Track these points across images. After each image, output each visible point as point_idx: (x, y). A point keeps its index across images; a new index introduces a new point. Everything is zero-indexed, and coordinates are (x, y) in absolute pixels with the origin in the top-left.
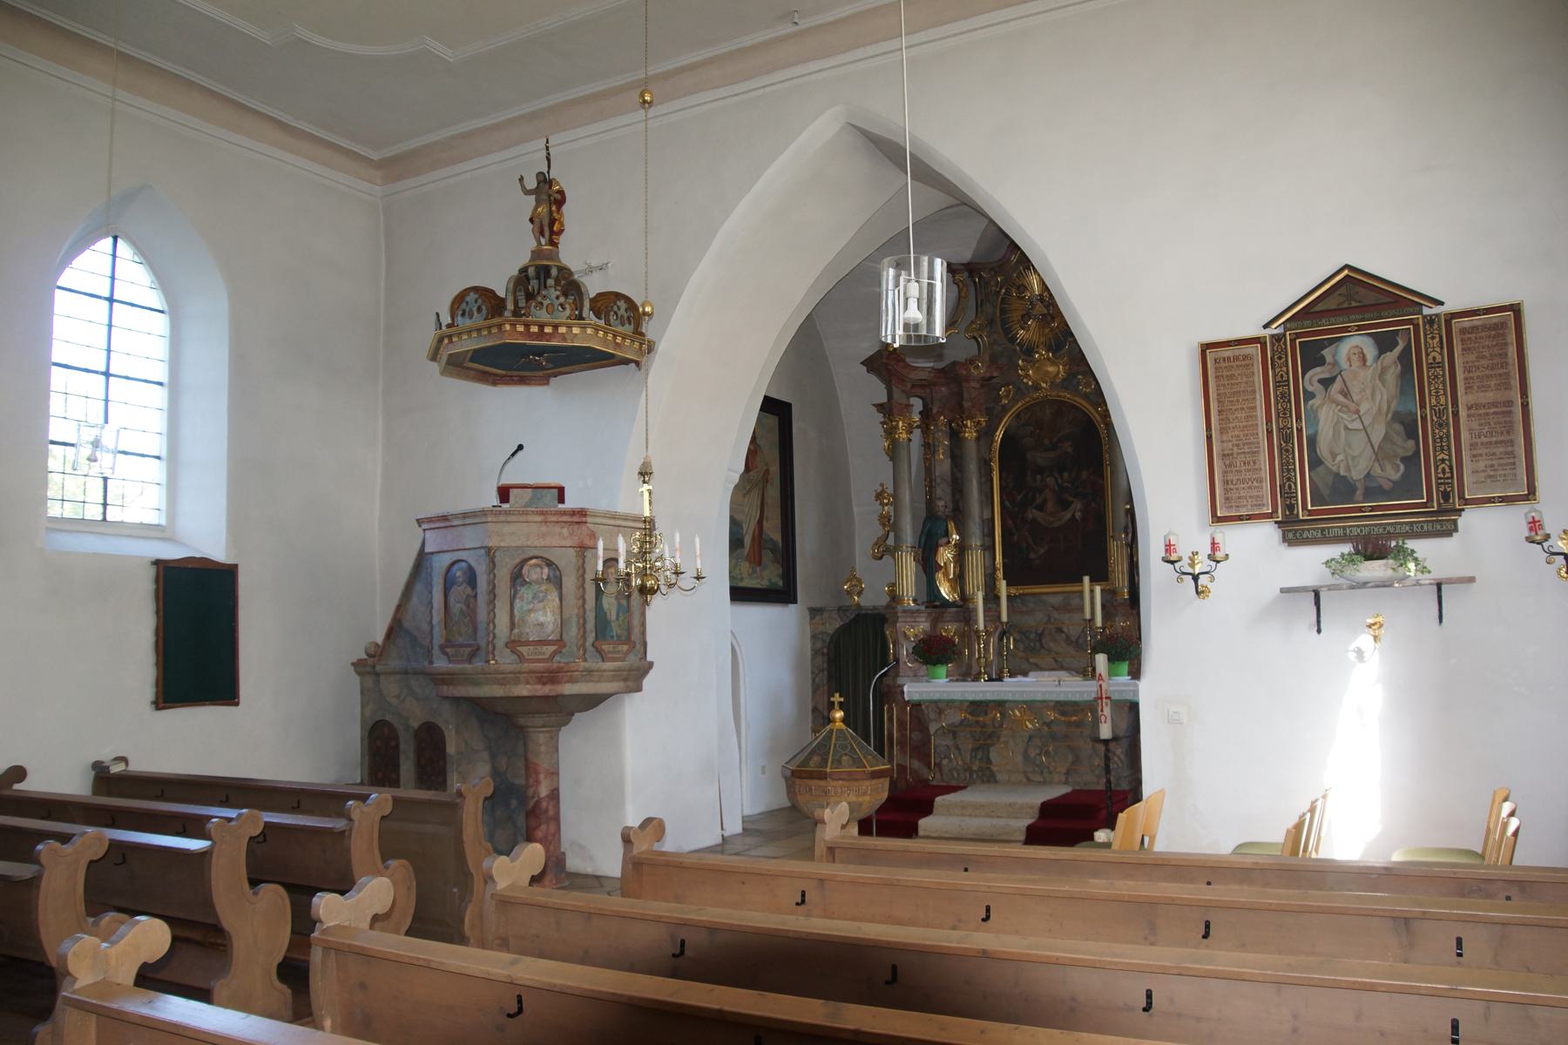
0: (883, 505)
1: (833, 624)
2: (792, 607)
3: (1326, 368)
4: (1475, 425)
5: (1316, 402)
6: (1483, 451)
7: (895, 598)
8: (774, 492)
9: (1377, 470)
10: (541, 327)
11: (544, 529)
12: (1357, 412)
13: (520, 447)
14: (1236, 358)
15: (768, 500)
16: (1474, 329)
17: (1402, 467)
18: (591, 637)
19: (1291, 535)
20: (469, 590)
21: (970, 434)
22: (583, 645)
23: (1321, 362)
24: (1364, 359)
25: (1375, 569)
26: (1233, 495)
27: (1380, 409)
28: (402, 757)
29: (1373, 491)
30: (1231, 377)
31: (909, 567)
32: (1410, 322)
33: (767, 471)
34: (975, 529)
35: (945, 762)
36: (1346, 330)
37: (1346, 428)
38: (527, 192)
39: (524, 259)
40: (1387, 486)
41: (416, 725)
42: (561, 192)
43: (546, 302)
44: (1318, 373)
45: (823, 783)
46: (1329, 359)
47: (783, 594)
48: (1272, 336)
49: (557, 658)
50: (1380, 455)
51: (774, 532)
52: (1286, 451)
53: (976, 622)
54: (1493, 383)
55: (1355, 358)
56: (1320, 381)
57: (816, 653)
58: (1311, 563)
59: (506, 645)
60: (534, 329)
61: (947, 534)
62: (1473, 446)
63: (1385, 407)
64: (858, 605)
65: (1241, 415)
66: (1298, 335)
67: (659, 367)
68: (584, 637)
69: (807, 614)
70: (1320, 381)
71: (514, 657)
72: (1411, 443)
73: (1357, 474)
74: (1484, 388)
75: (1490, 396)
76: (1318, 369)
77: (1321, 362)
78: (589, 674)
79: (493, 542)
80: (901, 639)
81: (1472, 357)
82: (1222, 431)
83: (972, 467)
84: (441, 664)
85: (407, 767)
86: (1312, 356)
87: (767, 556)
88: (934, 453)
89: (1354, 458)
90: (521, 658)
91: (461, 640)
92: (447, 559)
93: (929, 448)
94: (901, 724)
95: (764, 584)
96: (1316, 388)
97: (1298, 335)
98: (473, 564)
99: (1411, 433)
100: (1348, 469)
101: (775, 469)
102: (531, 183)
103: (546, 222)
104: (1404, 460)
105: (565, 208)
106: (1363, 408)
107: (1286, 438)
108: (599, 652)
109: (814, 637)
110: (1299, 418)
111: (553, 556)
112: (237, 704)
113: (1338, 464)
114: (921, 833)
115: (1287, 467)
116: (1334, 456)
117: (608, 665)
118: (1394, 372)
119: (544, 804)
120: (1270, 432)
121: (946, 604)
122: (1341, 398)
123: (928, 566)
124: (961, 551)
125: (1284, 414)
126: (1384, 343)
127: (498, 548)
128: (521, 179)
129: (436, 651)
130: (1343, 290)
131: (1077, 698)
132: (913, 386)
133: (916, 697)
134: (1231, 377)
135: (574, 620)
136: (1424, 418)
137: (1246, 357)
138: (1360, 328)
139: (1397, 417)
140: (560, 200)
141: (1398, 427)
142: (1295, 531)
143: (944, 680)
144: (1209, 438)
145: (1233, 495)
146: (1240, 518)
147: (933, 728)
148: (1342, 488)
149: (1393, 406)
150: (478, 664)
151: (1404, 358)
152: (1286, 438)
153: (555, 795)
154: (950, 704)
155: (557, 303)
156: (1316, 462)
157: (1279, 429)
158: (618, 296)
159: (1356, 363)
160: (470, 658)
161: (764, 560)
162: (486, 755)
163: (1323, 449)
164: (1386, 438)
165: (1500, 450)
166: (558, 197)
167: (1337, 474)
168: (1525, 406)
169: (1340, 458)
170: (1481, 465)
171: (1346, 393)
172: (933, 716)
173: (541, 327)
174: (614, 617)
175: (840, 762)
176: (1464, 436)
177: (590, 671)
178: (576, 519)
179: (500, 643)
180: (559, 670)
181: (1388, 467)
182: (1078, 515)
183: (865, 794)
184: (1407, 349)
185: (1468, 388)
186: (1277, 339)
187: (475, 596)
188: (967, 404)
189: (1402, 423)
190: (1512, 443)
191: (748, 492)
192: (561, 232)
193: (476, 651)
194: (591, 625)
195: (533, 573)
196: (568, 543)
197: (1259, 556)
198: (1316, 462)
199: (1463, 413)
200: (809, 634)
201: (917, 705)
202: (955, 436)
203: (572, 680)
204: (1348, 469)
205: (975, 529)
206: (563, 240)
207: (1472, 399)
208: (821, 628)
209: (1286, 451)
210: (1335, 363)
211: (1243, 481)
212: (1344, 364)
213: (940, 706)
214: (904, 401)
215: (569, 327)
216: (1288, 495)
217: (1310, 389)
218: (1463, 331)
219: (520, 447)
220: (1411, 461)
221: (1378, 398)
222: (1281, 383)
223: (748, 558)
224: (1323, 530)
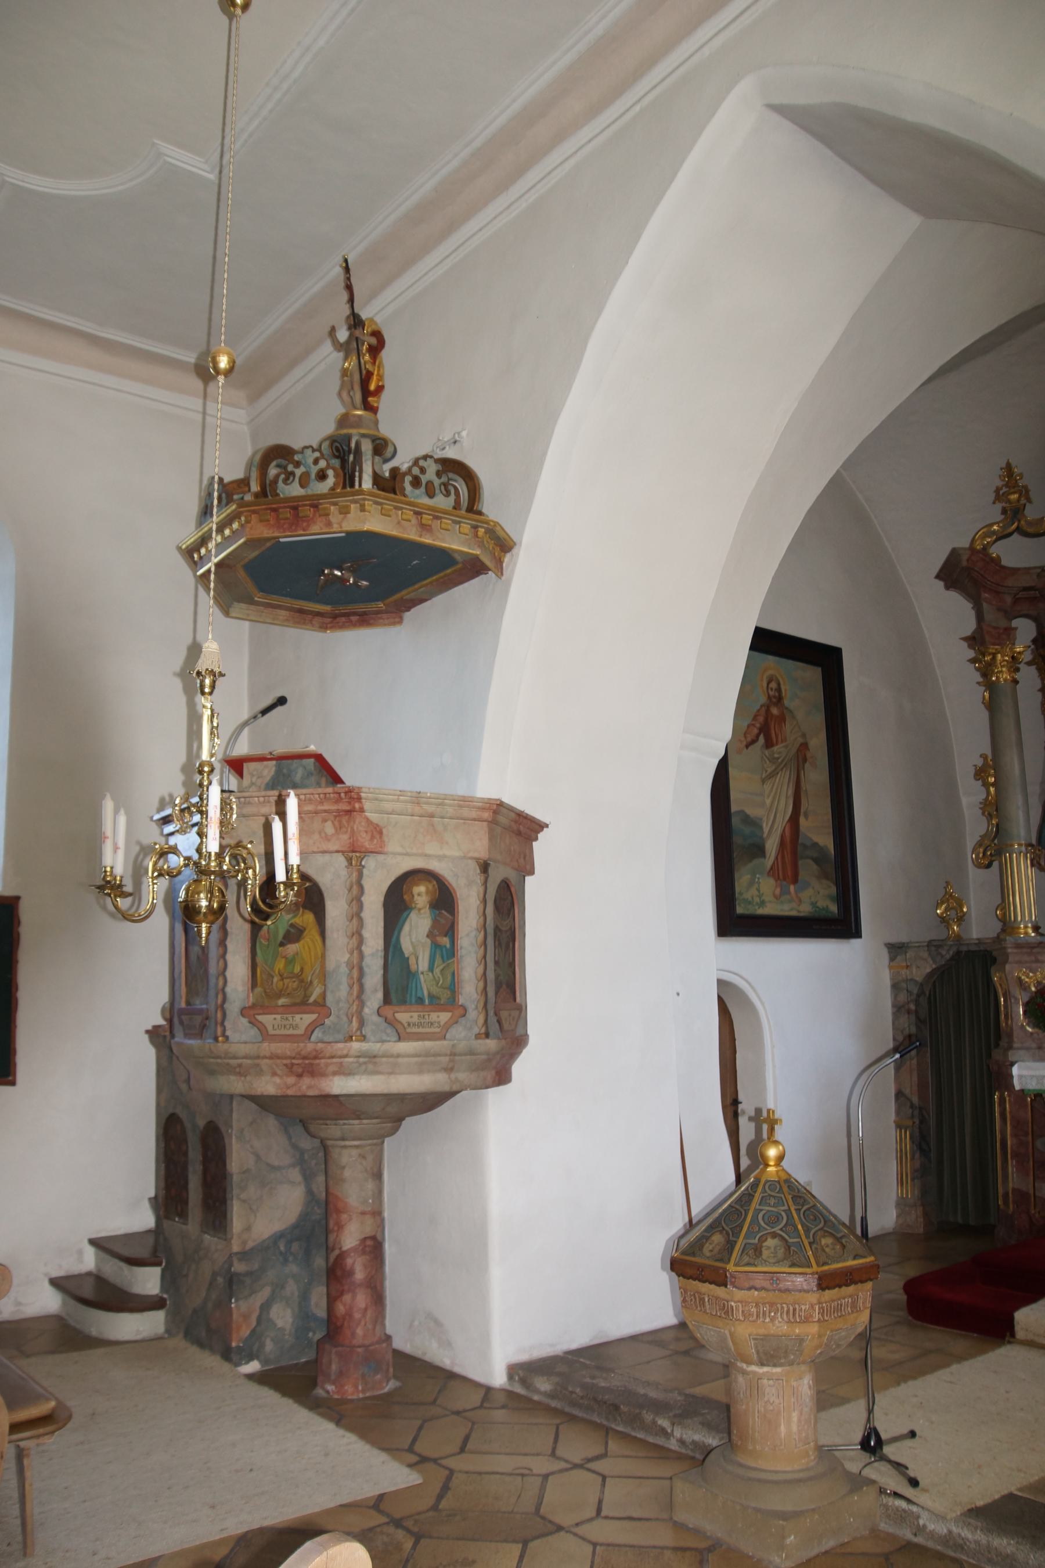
0: (986, 785)
1: (922, 969)
2: (855, 942)
7: (1008, 926)
8: (817, 776)
13: (282, 701)
15: (806, 786)
18: (374, 999)
22: (360, 1013)
28: (190, 1169)
33: (804, 746)
42: (377, 334)
43: (298, 472)
45: (720, 1291)
47: (841, 924)
49: (317, 1034)
51: (818, 831)
57: (898, 1009)
59: (243, 1012)
60: (287, 514)
64: (958, 938)
67: (522, 565)
68: (360, 998)
69: (885, 952)
71: (254, 1032)
78: (370, 1062)
80: (1016, 992)
87: (808, 869)
94: (1018, 1124)
95: (804, 909)
101: (818, 744)
105: (385, 354)
108: (391, 1022)
109: (895, 987)
112: (13, 1083)
114: (1020, 1334)
117: (404, 1047)
119: (349, 1261)
132: (1016, 601)
133: (1032, 1085)
135: (344, 969)
155: (314, 470)
161: (803, 875)
162: (295, 1174)
166: (373, 341)
174: (423, 965)
175: (758, 1251)
177: (373, 1057)
179: (233, 1007)
183: (807, 1320)
191: (772, 775)
192: (380, 389)
194: (374, 978)
196: (333, 846)
200: (887, 982)
203: (343, 1071)
206: (384, 403)
208: (904, 972)
214: (1003, 623)
223: (772, 872)
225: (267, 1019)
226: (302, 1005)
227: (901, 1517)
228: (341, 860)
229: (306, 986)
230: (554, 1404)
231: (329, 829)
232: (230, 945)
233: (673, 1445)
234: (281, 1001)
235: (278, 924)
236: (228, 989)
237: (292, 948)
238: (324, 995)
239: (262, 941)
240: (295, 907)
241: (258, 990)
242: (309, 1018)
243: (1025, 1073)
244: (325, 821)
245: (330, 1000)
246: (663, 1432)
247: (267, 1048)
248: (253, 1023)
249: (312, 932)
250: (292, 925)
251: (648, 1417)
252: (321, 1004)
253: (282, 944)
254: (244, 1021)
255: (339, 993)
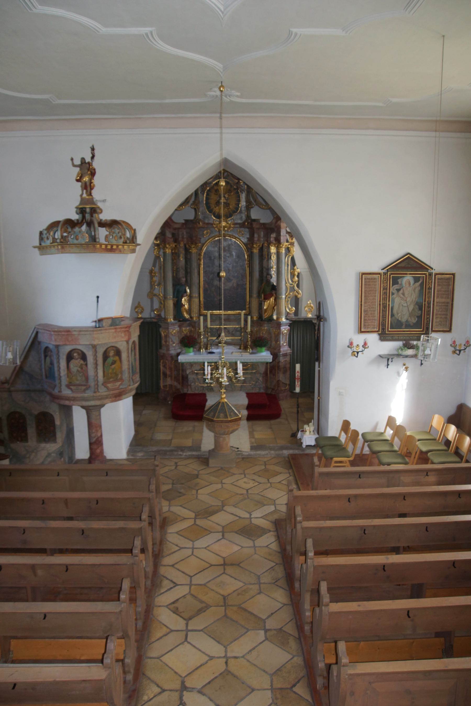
3: (398, 285)
4: (438, 308)
5: (394, 296)
6: (439, 316)
9: (410, 319)
10: (112, 246)
11: (115, 334)
12: (406, 300)
13: (98, 297)
14: (372, 279)
16: (441, 279)
17: (417, 319)
19: (382, 338)
20: (82, 362)
21: (194, 251)
23: (397, 283)
24: (410, 284)
25: (410, 352)
26: (367, 324)
27: (412, 301)
29: (408, 326)
30: (369, 285)
31: (170, 304)
32: (424, 274)
34: (195, 289)
35: (193, 384)
36: (406, 274)
37: (402, 305)
38: (74, 166)
39: (77, 202)
40: (412, 324)
41: (36, 413)
42: (94, 169)
44: (396, 287)
46: (400, 283)
48: (384, 273)
50: (411, 315)
52: (384, 311)
53: (200, 329)
54: (444, 296)
55: (407, 283)
56: (397, 290)
58: (389, 347)
59: (103, 384)
60: (109, 247)
61: (186, 292)
62: (436, 314)
63: (414, 300)
65: (371, 298)
66: (392, 274)
70: (397, 290)
71: (106, 389)
72: (420, 312)
73: (404, 320)
74: (442, 298)
75: (443, 300)
76: (396, 286)
77: (397, 283)
79: (96, 342)
81: (440, 287)
82: (365, 303)
83: (194, 265)
84: (66, 392)
85: (32, 431)
86: (395, 281)
88: (179, 257)
89: (403, 315)
90: (108, 388)
91: (78, 382)
92: (68, 348)
93: (175, 255)
96: (395, 291)
97: (392, 274)
98: (85, 351)
99: (421, 309)
100: (401, 318)
102: (78, 162)
103: (88, 184)
104: (418, 317)
105: (96, 177)
106: (408, 300)
107: (385, 307)
110: (389, 301)
111: (118, 345)
113: (398, 316)
115: (384, 316)
116: (398, 314)
118: (417, 290)
120: (380, 305)
121: (185, 320)
122: (402, 296)
123: (178, 305)
124: (190, 297)
125: (385, 299)
126: (416, 280)
127: (98, 345)
128: (72, 159)
129: (63, 387)
130: (407, 261)
131: (248, 361)
133: (183, 361)
134: (369, 285)
135: (127, 370)
136: (425, 305)
137: (375, 279)
138: (410, 274)
139: (417, 303)
140: (93, 174)
141: (417, 307)
142: (384, 337)
143: (192, 354)
144: (361, 305)
145: (367, 324)
146: (368, 332)
147: (188, 372)
148: (398, 324)
149: (417, 299)
150: (89, 394)
151: (422, 285)
152: (385, 307)
153: (101, 436)
154: (196, 363)
156: (393, 315)
157: (383, 304)
158: (129, 226)
159: (407, 285)
160: (84, 391)
163: (395, 311)
164: (413, 310)
165: (443, 316)
167: (398, 320)
168: (452, 304)
169: (399, 314)
170: (438, 320)
171: (403, 294)
172: (188, 367)
173: (112, 246)
176: (435, 311)
178: (127, 329)
179: (100, 383)
180: (124, 391)
181: (413, 319)
182: (235, 285)
184: (423, 282)
185: (438, 297)
186: (385, 274)
187: (86, 365)
188: (194, 238)
189: (418, 305)
190: (447, 315)
193: (88, 387)
195: (112, 353)
197: (377, 346)
198: (393, 315)
199: (435, 304)
201: (183, 364)
202: (187, 251)
204: (401, 318)
205: (195, 289)
206: (93, 192)
207: (438, 300)
209: (384, 311)
210: (401, 284)
211: (370, 320)
212: (404, 285)
213: (191, 364)
215: (123, 246)
216: (384, 325)
217: (393, 292)
218: (439, 279)
219: (98, 297)
220: (420, 317)
221: (412, 296)
222: (385, 289)
224: (392, 337)
225: (109, 385)
226: (116, 380)
227: (239, 454)
228: (125, 343)
229: (116, 374)
230: (145, 457)
231: (123, 335)
232: (99, 368)
233: (183, 457)
234: (111, 380)
235: (110, 360)
236: (99, 379)
237: (113, 366)
238: (121, 377)
239: (106, 365)
240: (114, 356)
241: (105, 378)
242: (119, 383)
243: (182, 358)
244: (122, 333)
245: (124, 378)
246: (180, 455)
247: (112, 392)
248: (105, 387)
249: (118, 362)
250: (113, 360)
251: (176, 453)
252: (121, 379)
253: (111, 365)
254: (103, 387)
255: (126, 376)
